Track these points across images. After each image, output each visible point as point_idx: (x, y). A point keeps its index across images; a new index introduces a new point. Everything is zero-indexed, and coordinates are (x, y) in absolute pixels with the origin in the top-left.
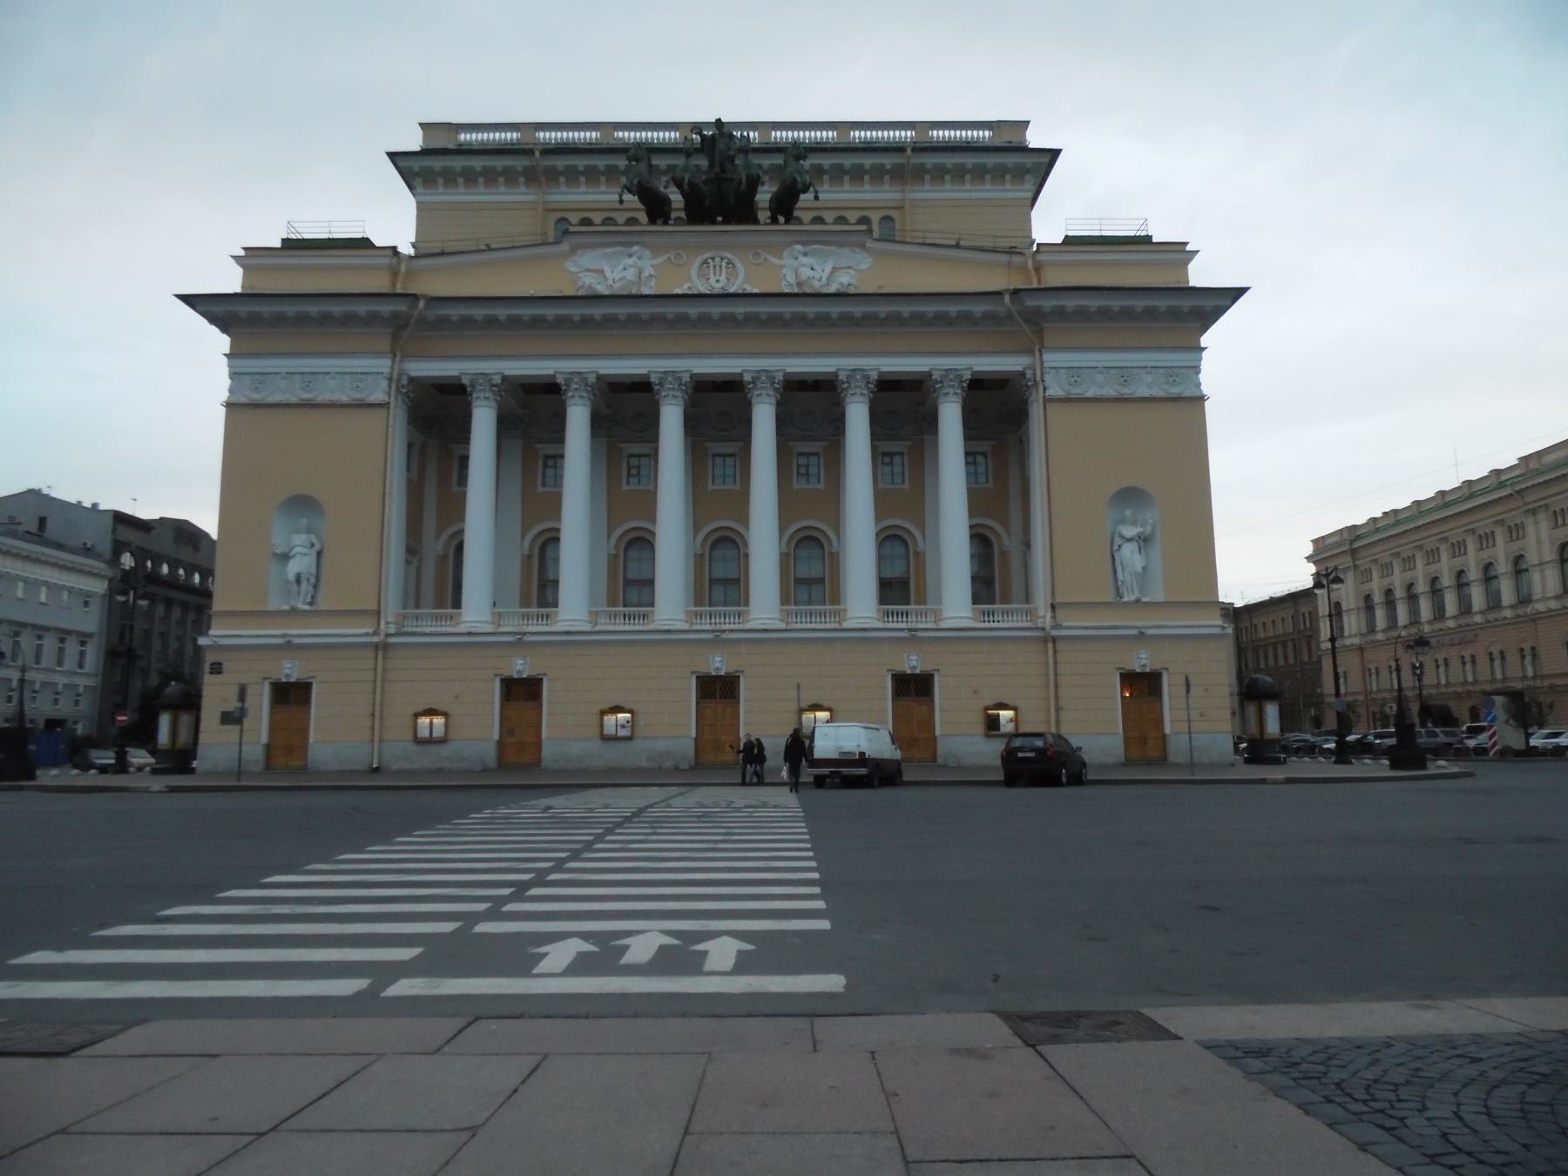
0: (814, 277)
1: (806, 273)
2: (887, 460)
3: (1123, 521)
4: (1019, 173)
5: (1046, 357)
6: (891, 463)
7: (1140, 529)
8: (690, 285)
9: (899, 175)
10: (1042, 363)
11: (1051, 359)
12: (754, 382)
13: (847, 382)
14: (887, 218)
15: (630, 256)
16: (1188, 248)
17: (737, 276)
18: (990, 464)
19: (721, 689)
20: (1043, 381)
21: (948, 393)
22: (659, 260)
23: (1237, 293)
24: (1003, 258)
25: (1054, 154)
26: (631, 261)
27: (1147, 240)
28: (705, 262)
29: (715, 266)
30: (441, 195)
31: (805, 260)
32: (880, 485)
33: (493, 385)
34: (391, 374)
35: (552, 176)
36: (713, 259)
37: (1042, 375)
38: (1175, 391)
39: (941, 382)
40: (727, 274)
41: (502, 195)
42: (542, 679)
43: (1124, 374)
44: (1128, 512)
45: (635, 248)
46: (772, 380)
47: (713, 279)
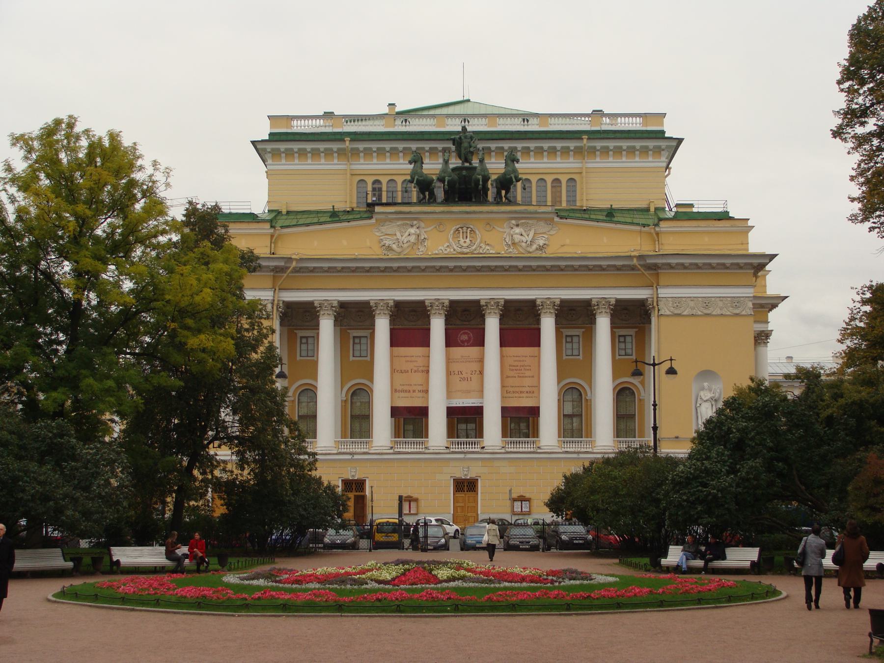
0: (522, 241)
1: (517, 238)
2: (569, 339)
3: (703, 389)
4: (658, 151)
5: (659, 290)
6: (572, 342)
7: (713, 395)
8: (448, 244)
9: (579, 151)
10: (658, 294)
11: (663, 292)
12: (486, 305)
13: (542, 305)
14: (572, 180)
15: (412, 226)
16: (750, 223)
17: (477, 239)
18: (634, 343)
19: (467, 486)
20: (658, 305)
21: (602, 312)
22: (429, 229)
23: (772, 257)
24: (638, 228)
25: (680, 141)
26: (412, 230)
27: (724, 216)
28: (457, 230)
29: (463, 232)
30: (283, 165)
31: (517, 230)
32: (565, 357)
33: (332, 307)
34: (274, 300)
35: (355, 153)
36: (462, 228)
37: (657, 302)
38: (737, 311)
39: (598, 305)
40: (470, 237)
41: (323, 165)
42: (365, 480)
43: (707, 302)
44: (706, 384)
45: (415, 222)
46: (497, 304)
47: (462, 241)
